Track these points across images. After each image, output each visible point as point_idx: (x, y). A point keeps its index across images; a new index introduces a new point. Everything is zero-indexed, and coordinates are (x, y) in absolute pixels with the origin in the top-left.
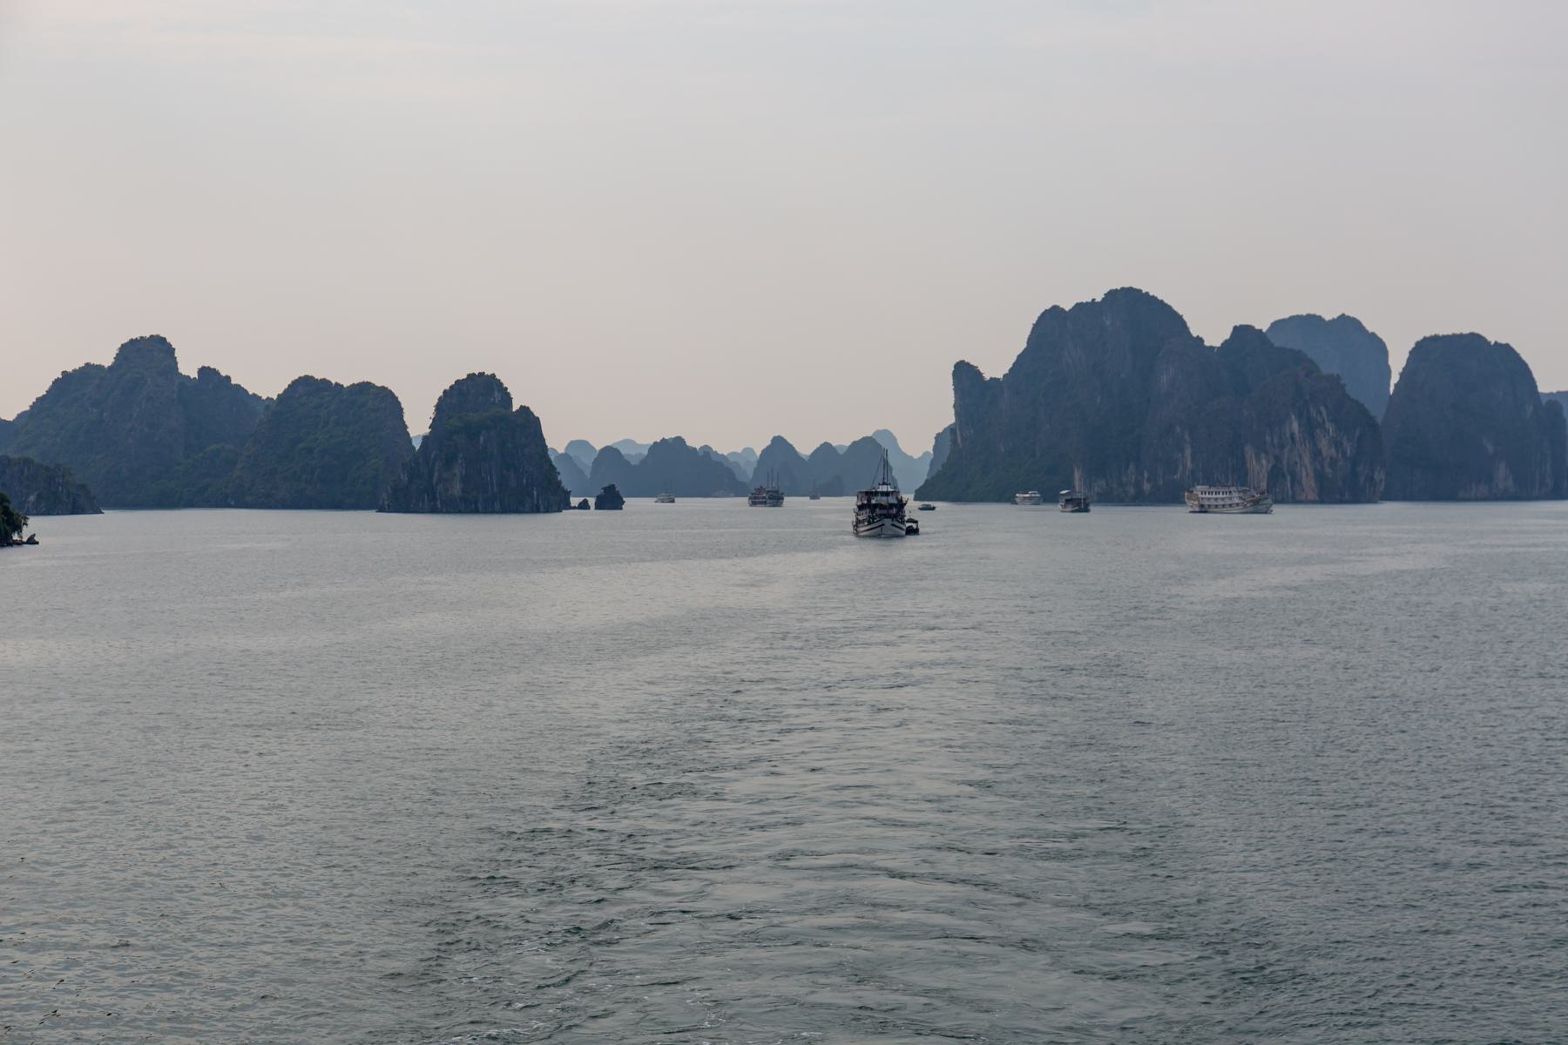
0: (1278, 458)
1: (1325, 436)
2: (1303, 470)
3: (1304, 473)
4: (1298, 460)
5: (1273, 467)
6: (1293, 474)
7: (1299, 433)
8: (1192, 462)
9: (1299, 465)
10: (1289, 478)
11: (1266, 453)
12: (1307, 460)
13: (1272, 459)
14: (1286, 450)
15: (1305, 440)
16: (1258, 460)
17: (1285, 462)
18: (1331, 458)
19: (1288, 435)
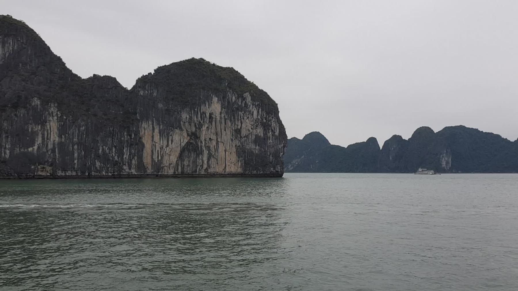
0: (194, 136)
1: (248, 118)
2: (221, 145)
3: (221, 148)
4: (214, 137)
5: (188, 144)
6: (208, 148)
7: (221, 113)
8: (60, 136)
9: (214, 143)
10: (206, 153)
11: (181, 129)
12: (227, 136)
13: (185, 134)
14: (204, 128)
15: (225, 119)
16: (165, 134)
17: (203, 138)
18: (256, 135)
19: (208, 115)
